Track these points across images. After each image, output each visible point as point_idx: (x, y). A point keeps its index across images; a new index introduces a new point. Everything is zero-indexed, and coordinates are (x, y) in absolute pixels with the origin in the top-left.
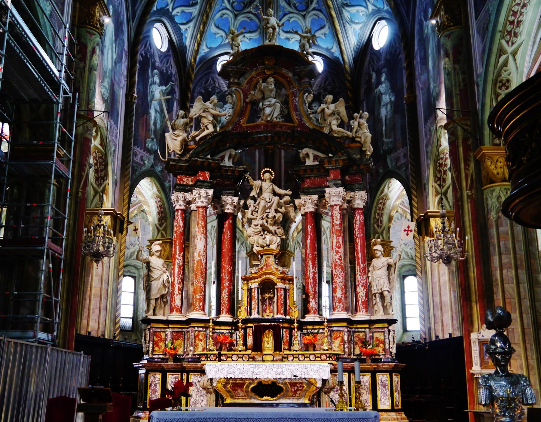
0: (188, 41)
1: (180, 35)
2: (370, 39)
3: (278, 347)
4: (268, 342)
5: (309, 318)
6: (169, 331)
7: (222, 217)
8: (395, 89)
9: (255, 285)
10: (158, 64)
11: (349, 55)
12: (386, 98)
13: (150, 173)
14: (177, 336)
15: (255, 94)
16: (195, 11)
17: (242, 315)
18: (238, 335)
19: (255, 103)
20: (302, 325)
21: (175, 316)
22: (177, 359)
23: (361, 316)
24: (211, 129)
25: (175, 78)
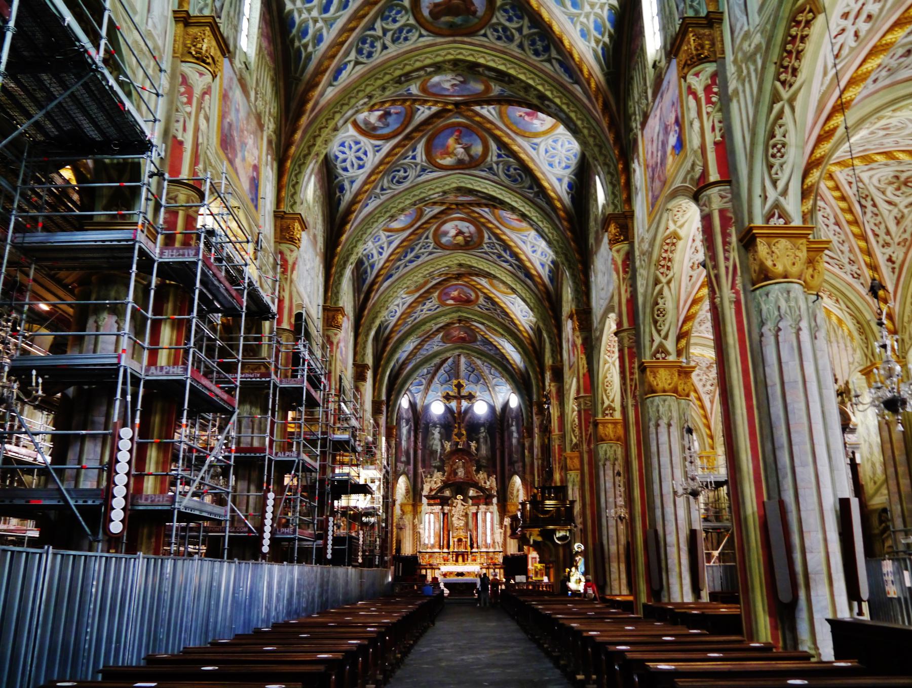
0: (418, 401)
1: (414, 397)
2: (508, 401)
3: (463, 561)
4: (460, 559)
5: (474, 550)
6: (427, 556)
7: (444, 514)
8: (518, 432)
9: (456, 540)
10: (405, 416)
11: (498, 408)
12: (515, 435)
13: (404, 473)
14: (430, 557)
15: (455, 467)
16: (422, 387)
17: (451, 550)
18: (450, 556)
19: (455, 470)
20: (471, 553)
21: (429, 550)
22: (430, 565)
23: (491, 550)
24: (440, 484)
25: (412, 420)
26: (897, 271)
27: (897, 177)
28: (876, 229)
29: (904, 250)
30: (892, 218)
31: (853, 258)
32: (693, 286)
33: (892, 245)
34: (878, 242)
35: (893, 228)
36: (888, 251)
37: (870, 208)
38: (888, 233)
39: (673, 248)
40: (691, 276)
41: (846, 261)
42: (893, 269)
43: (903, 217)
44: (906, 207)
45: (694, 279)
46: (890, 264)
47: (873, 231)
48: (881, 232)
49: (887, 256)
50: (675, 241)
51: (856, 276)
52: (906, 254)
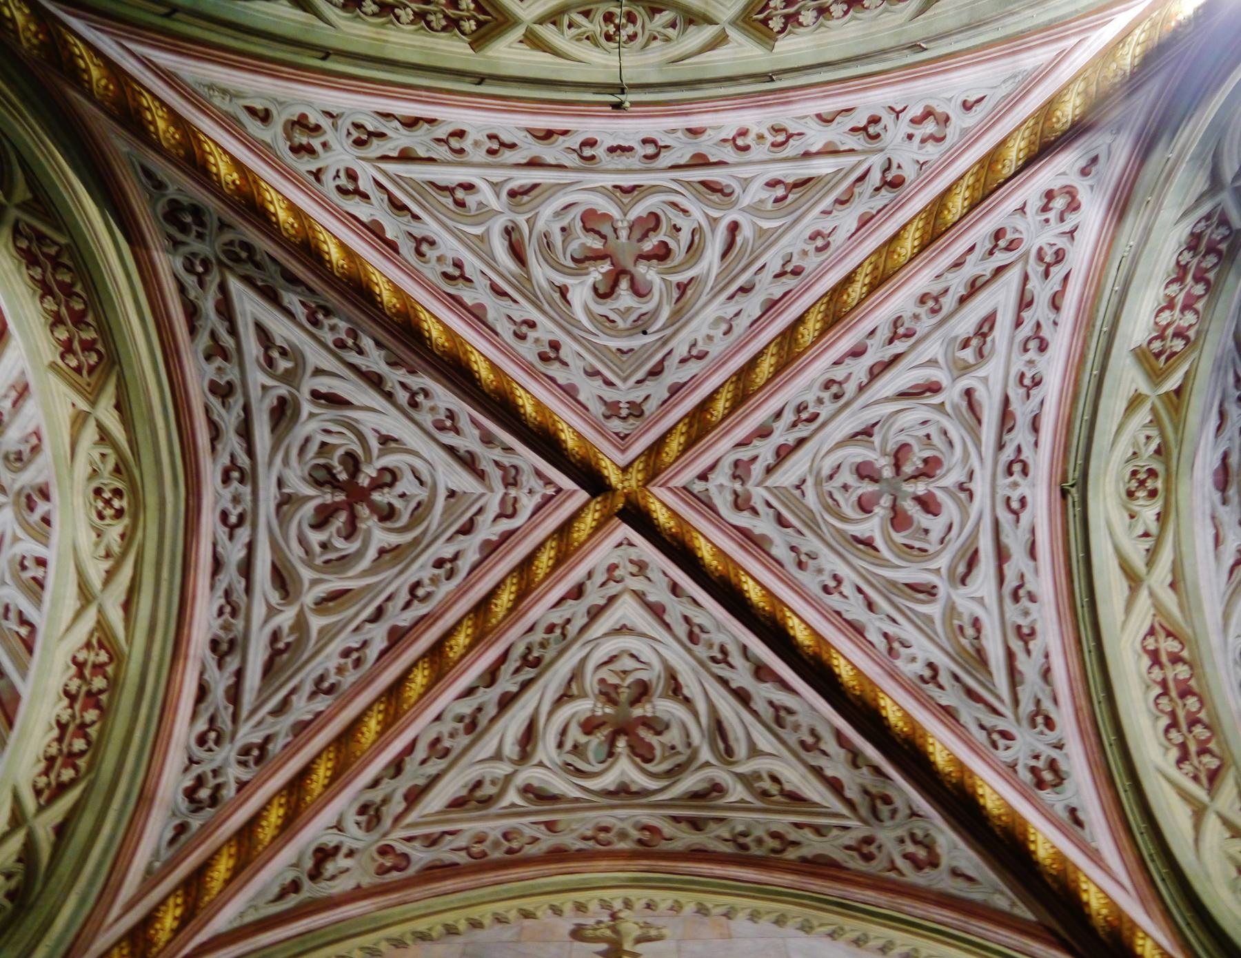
26: (292, 901)
27: (643, 691)
28: (421, 752)
29: (367, 880)
30: (473, 774)
31: (275, 748)
32: (229, 123)
33: (375, 835)
34: (375, 783)
35: (436, 800)
36: (355, 836)
37: (489, 697)
38: (414, 797)
39: (438, 21)
40: (265, 117)
41: (248, 734)
42: (295, 886)
43: (487, 801)
44: (527, 790)
45: (254, 127)
46: (309, 864)
47: (410, 748)
48: (413, 775)
49: (331, 839)
50: (470, 26)
51: (204, 794)
52: (358, 894)
